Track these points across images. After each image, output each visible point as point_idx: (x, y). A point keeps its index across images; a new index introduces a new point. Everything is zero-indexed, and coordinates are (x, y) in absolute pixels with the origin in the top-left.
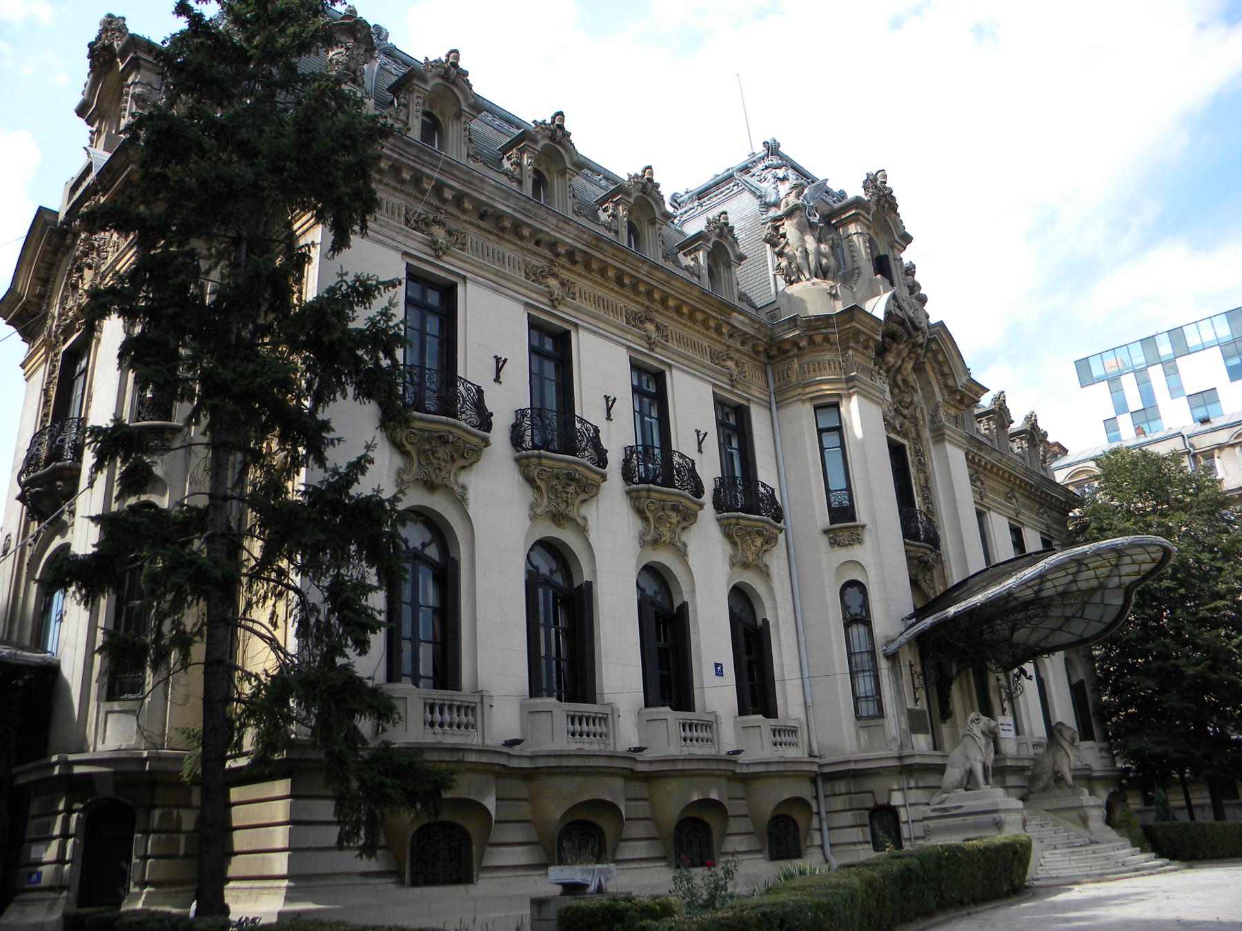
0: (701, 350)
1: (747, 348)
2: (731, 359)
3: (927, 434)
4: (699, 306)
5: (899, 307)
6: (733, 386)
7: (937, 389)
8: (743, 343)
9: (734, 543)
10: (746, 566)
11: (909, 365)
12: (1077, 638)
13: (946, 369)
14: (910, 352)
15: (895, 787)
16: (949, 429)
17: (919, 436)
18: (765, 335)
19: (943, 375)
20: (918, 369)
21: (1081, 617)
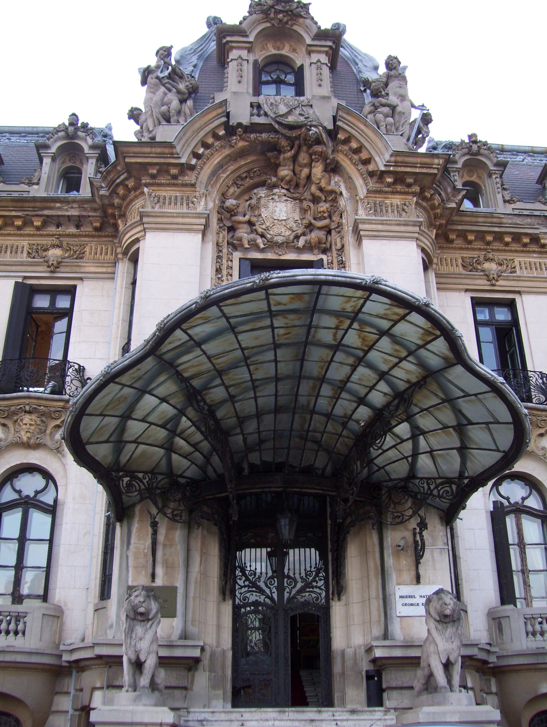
0: (15, 250)
1: (87, 229)
2: (54, 246)
3: (350, 239)
4: (14, 213)
5: (266, 114)
6: (52, 272)
7: (359, 182)
8: (78, 227)
9: (4, 425)
10: (27, 446)
11: (318, 170)
12: (498, 456)
13: (364, 155)
14: (311, 155)
15: (98, 685)
16: (370, 222)
17: (343, 246)
18: (95, 210)
19: (367, 162)
20: (333, 168)
21: (471, 423)
